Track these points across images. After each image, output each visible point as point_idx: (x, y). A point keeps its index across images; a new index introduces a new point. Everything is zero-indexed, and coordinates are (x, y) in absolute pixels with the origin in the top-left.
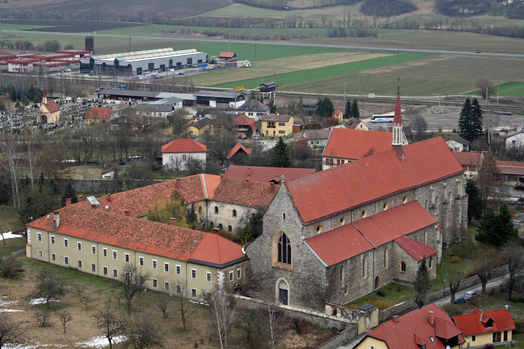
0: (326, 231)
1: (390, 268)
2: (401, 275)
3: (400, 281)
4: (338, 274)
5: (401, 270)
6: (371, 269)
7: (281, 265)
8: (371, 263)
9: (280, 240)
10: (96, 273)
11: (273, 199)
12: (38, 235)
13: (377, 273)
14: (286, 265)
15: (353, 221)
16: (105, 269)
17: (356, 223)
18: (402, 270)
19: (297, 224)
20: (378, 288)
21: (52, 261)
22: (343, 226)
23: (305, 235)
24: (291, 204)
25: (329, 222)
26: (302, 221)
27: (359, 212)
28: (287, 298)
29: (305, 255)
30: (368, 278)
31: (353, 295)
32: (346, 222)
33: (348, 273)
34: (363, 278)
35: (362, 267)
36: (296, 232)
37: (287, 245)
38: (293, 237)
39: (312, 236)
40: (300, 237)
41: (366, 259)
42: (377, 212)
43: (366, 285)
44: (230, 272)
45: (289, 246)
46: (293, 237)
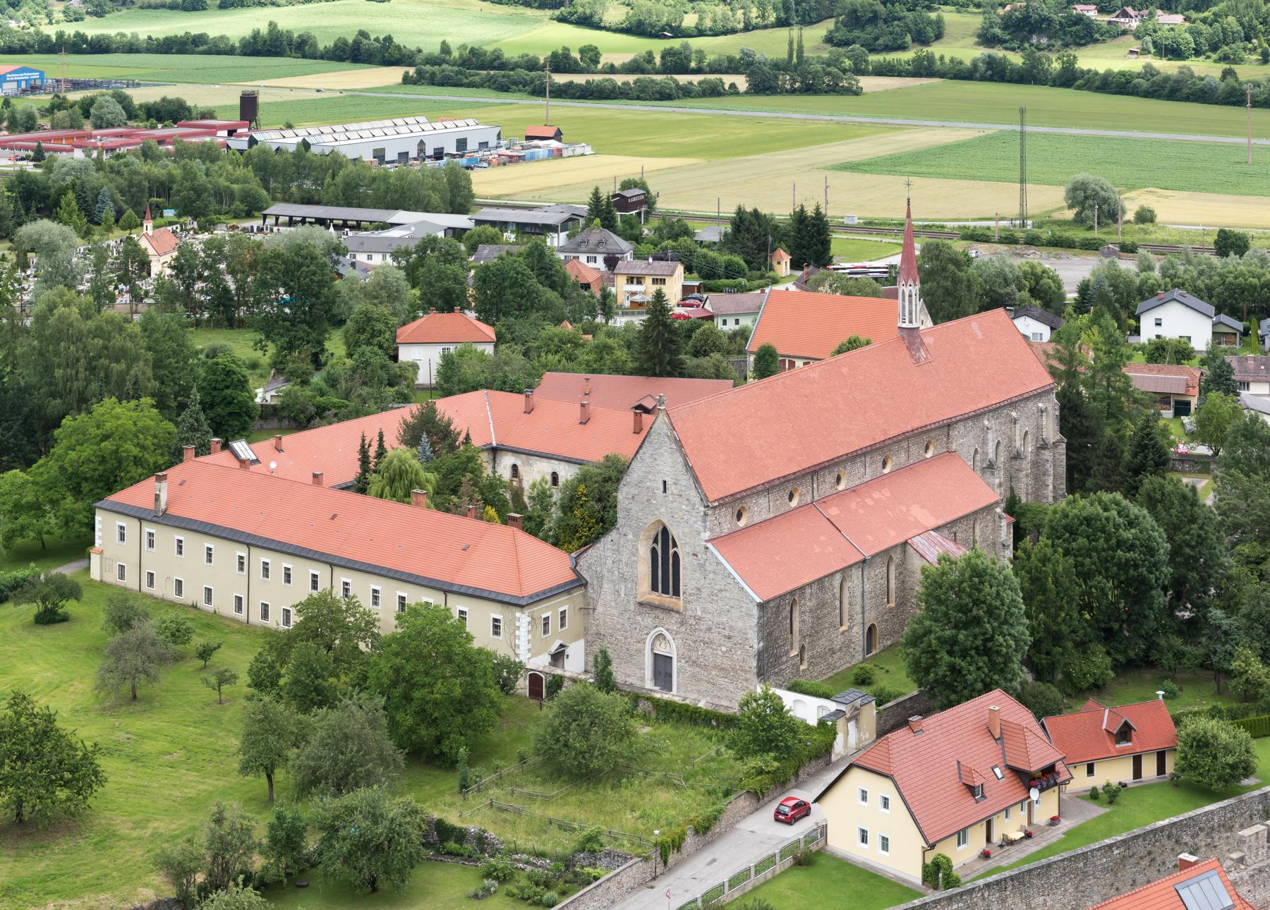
0: (757, 520)
1: (899, 605)
6: (858, 608)
7: (656, 598)
8: (858, 594)
9: (656, 541)
10: (242, 616)
12: (117, 529)
13: (871, 617)
14: (668, 600)
15: (816, 498)
16: (265, 607)
19: (694, 505)
21: (145, 588)
22: (795, 509)
23: (711, 530)
24: (680, 459)
25: (763, 501)
26: (704, 498)
27: (830, 479)
29: (711, 576)
30: (850, 628)
31: (818, 669)
35: (838, 603)
37: (671, 551)
39: (726, 531)
40: (699, 533)
41: (847, 584)
42: (867, 477)
43: (848, 644)
44: (544, 616)
45: (676, 554)
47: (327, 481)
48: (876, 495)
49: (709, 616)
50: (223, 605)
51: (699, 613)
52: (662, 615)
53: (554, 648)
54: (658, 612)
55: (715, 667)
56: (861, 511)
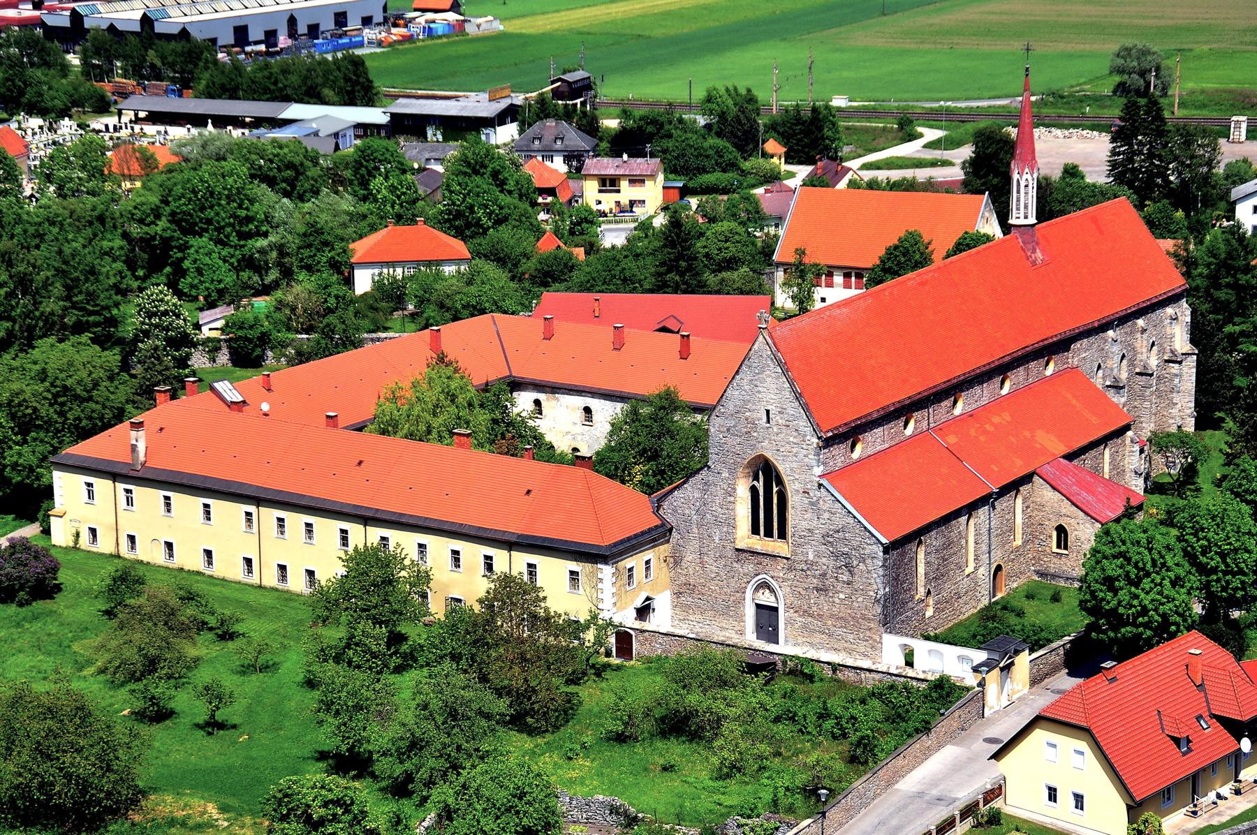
0: (870, 451)
1: (1025, 542)
2: (1055, 560)
3: (1054, 576)
4: (910, 561)
5: (1055, 550)
6: (984, 548)
7: (759, 543)
8: (984, 531)
10: (254, 579)
11: (737, 373)
14: (774, 545)
16: (282, 568)
17: (939, 429)
18: (1059, 546)
20: (999, 596)
22: (911, 437)
23: (824, 464)
28: (776, 629)
29: (826, 515)
32: (915, 428)
33: (932, 558)
34: (967, 572)
35: (963, 542)
36: (801, 456)
38: (792, 469)
41: (972, 522)
42: (984, 401)
44: (628, 566)
46: (792, 469)
47: (342, 422)
48: (996, 420)
49: (824, 560)
50: (228, 567)
51: (811, 557)
52: (766, 561)
53: (639, 603)
54: (760, 559)
55: (832, 616)
56: (982, 439)
